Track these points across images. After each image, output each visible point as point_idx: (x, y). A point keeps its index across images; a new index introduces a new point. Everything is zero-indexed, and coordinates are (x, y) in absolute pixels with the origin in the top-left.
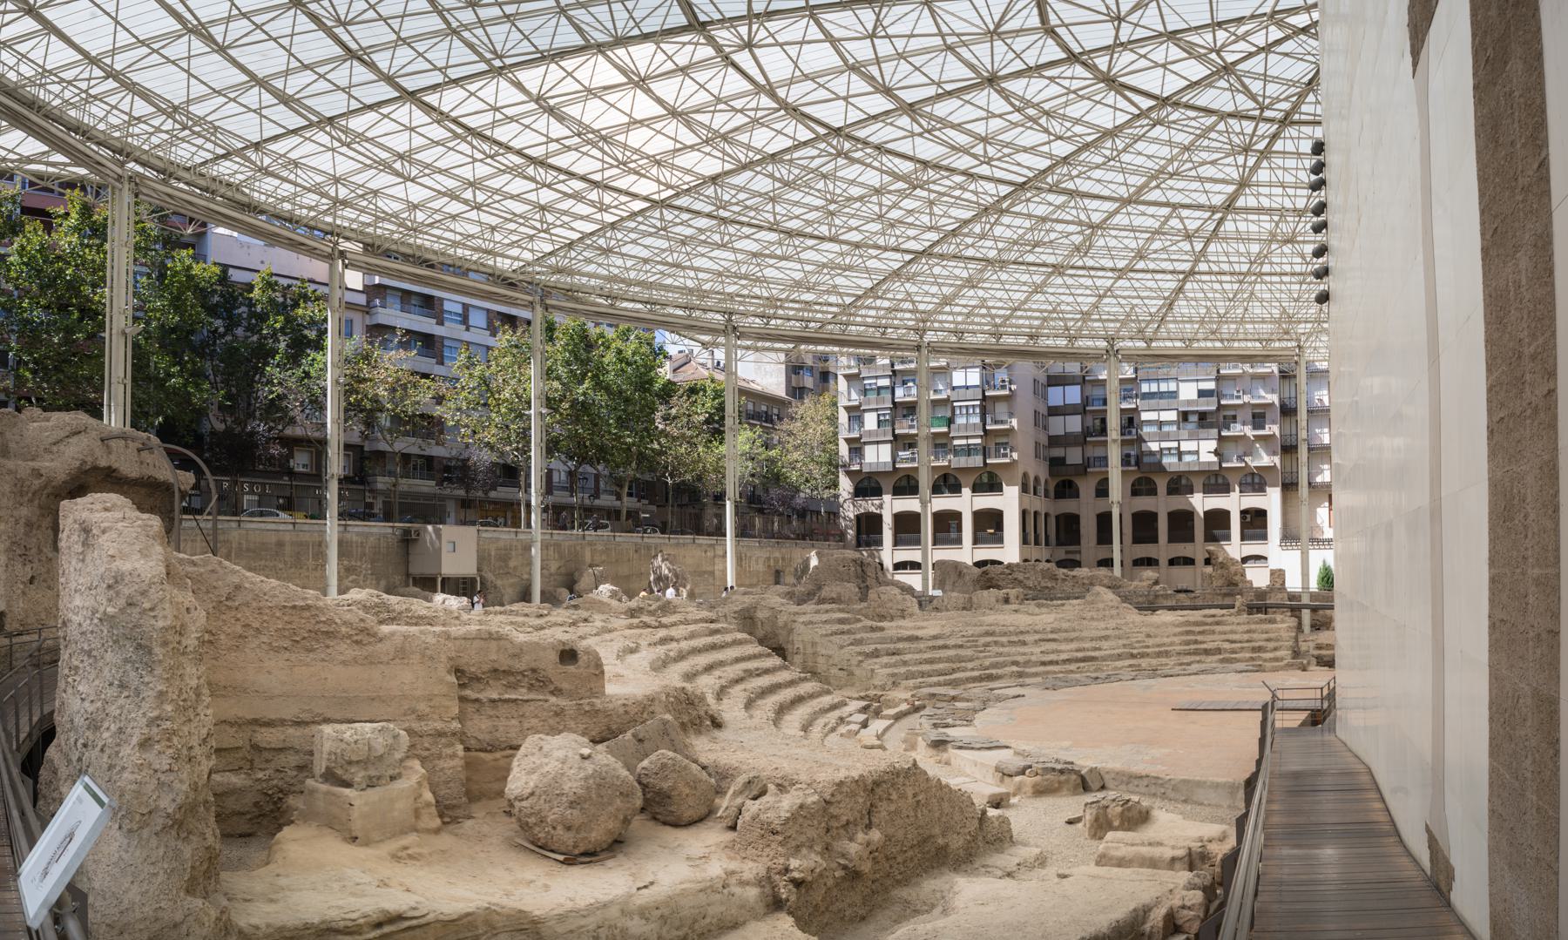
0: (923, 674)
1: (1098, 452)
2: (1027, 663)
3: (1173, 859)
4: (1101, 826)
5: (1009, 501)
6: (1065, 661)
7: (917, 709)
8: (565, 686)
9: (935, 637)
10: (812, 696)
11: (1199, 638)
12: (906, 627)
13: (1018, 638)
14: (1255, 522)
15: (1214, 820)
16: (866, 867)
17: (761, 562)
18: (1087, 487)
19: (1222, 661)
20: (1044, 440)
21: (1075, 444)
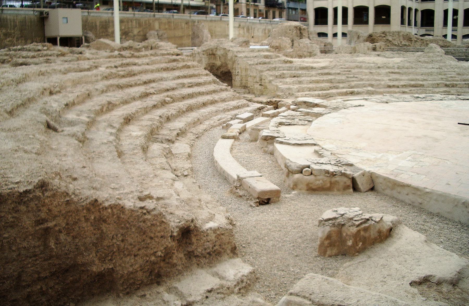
0: (310, 90)
9: (323, 68)
12: (307, 62)
17: (260, 30)
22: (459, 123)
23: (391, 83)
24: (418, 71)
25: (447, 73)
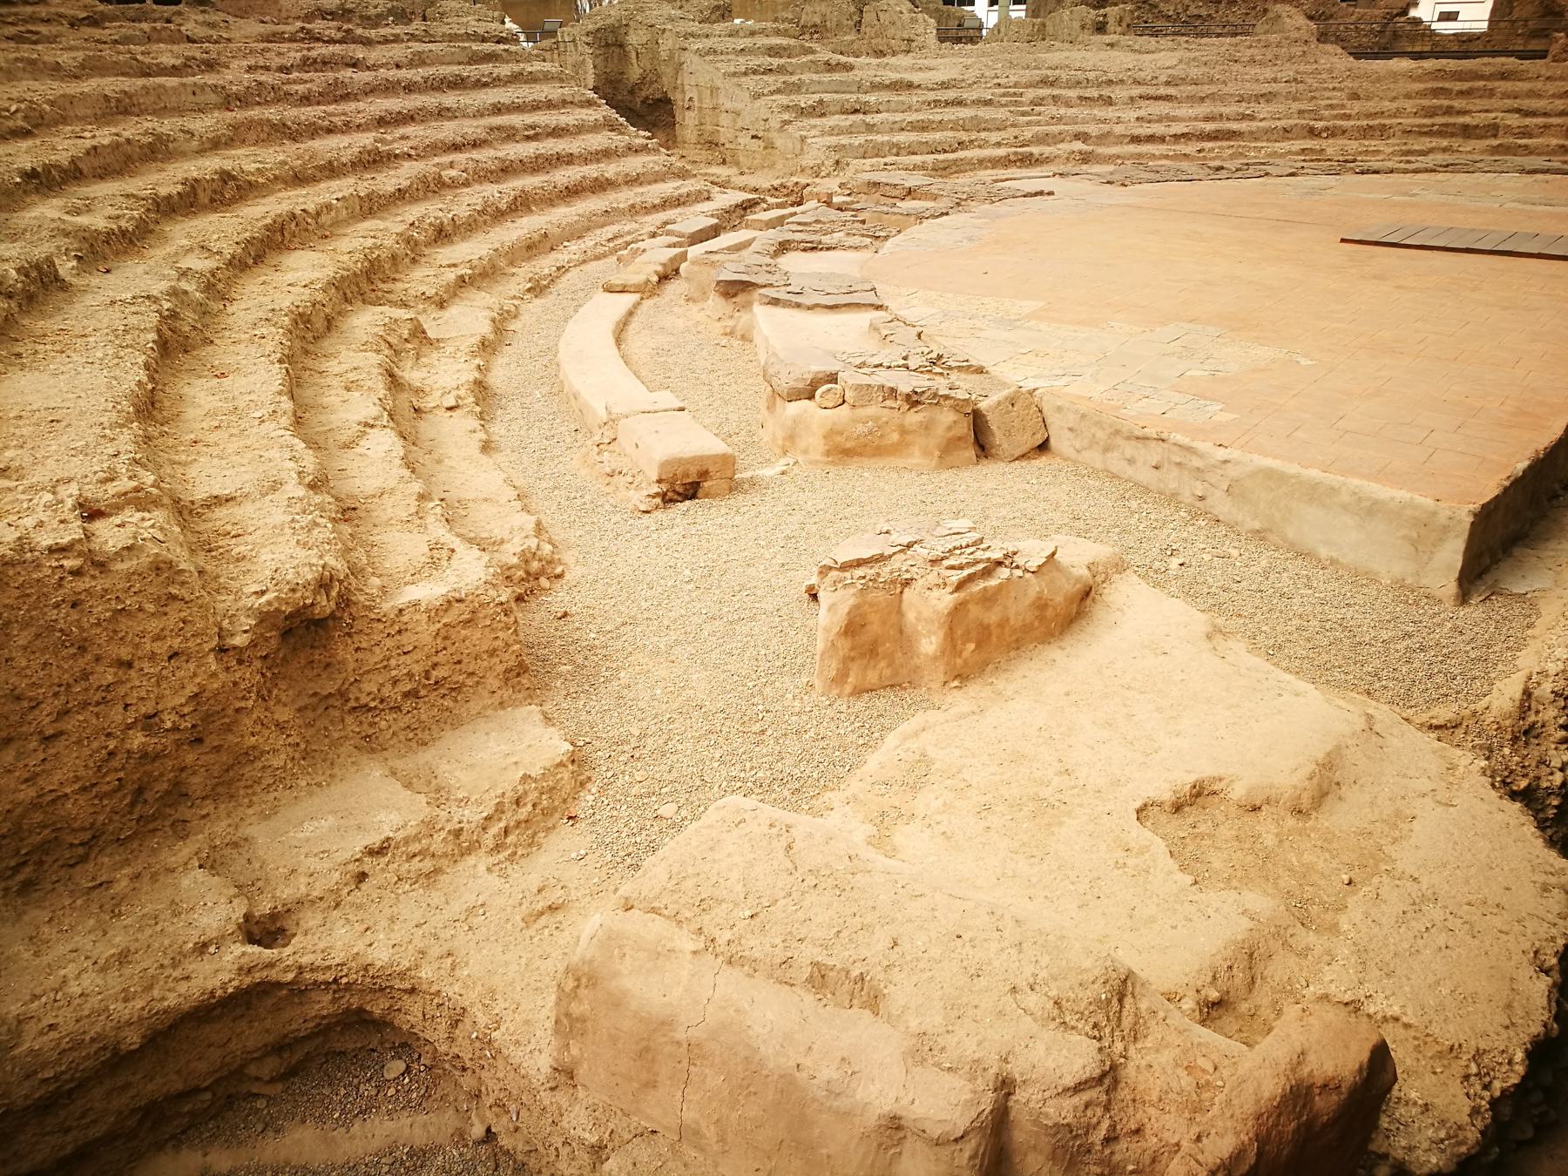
0: (898, 149)
2: (1103, 138)
6: (1177, 137)
9: (944, 86)
11: (1458, 104)
19: (1495, 150)
22: (1343, 240)
23: (1144, 130)
25: (1317, 94)
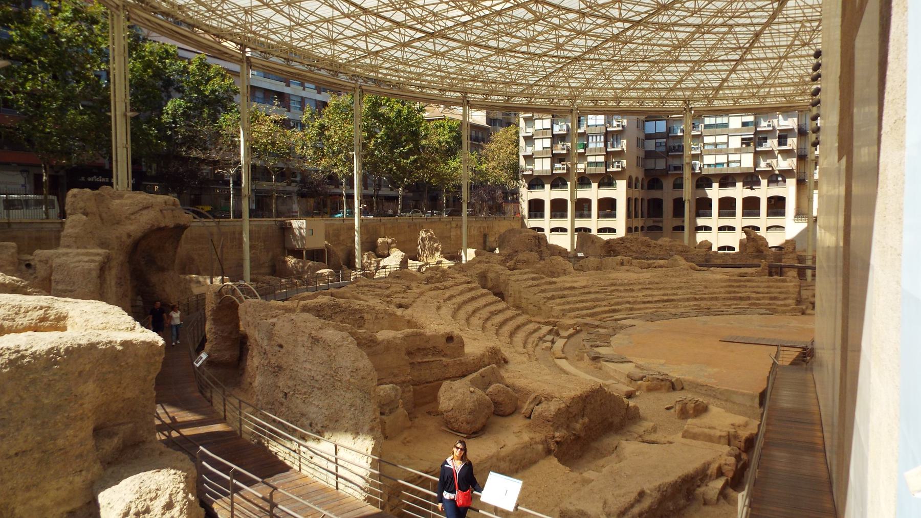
0: (578, 309)
1: (676, 163)
2: (635, 302)
3: (720, 437)
4: (684, 414)
5: (619, 192)
6: (656, 302)
7: (578, 332)
8: (448, 352)
9: (584, 287)
10: (524, 325)
11: (737, 290)
13: (629, 287)
14: (777, 205)
15: (741, 414)
16: (583, 434)
18: (668, 184)
20: (642, 154)
21: (662, 157)
24: (668, 285)
